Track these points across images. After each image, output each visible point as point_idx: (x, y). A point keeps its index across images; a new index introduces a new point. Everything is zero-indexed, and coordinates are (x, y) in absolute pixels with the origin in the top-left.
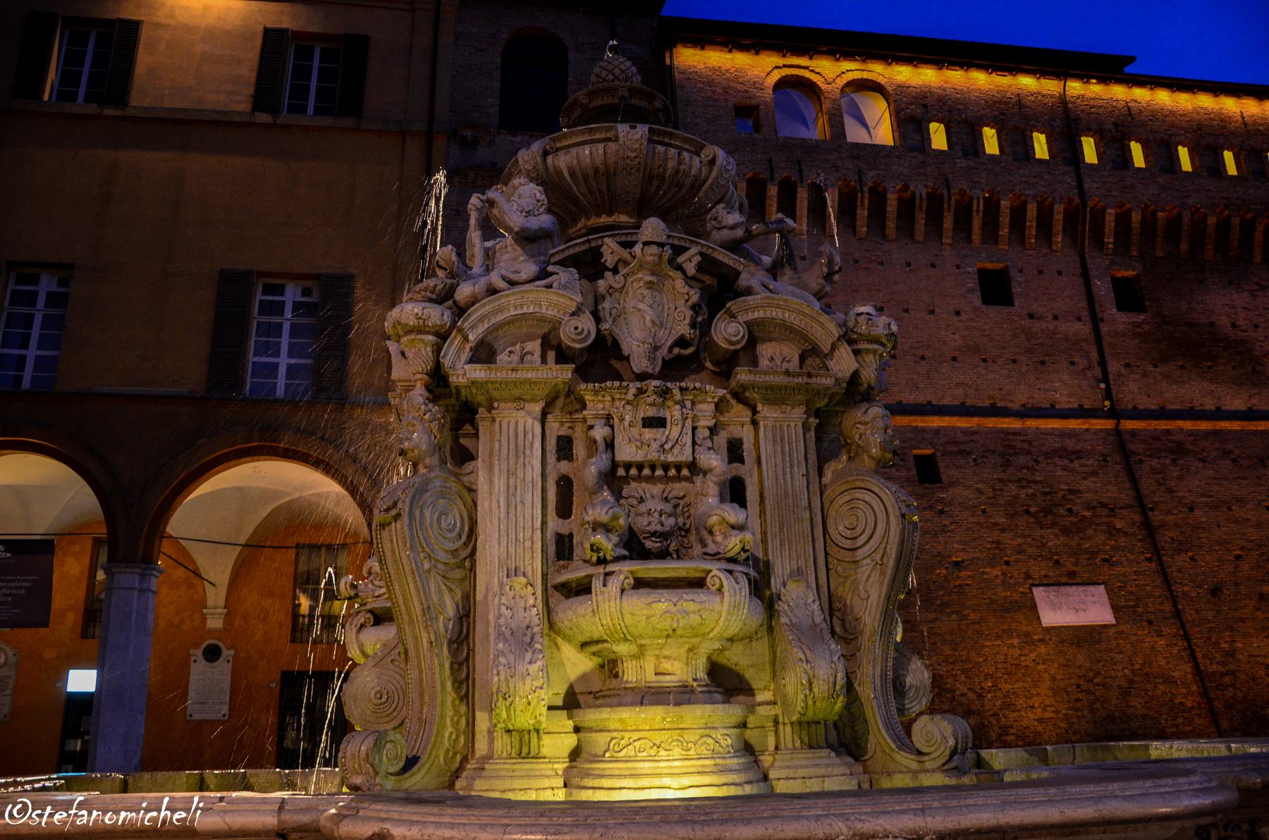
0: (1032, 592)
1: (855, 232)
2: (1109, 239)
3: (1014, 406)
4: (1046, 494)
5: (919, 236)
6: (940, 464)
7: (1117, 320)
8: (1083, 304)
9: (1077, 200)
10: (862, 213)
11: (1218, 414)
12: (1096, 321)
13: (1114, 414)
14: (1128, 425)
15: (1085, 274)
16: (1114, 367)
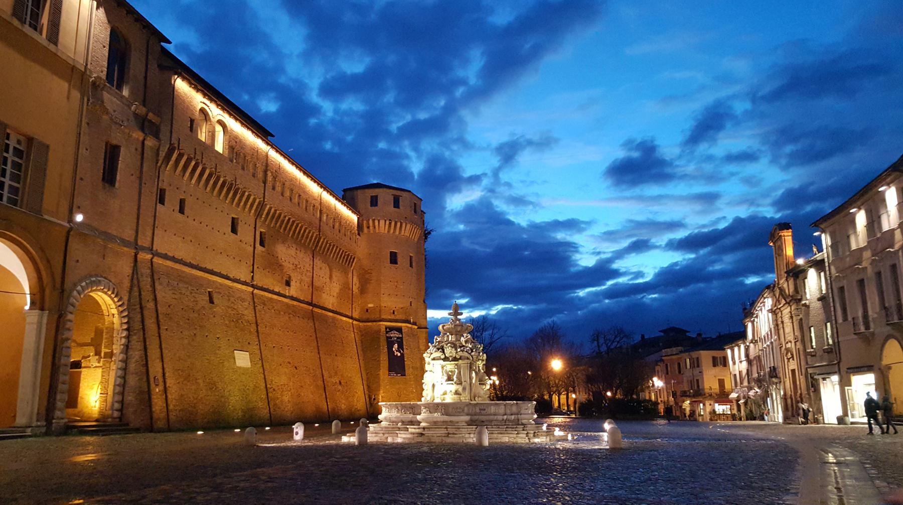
0: (234, 353)
1: (206, 189)
2: (263, 216)
3: (231, 276)
4: (237, 314)
5: (221, 198)
6: (214, 296)
7: (259, 248)
8: (253, 240)
9: (262, 199)
10: (212, 182)
11: (273, 292)
12: (254, 248)
13: (253, 286)
14: (256, 291)
15: (255, 228)
16: (255, 267)
